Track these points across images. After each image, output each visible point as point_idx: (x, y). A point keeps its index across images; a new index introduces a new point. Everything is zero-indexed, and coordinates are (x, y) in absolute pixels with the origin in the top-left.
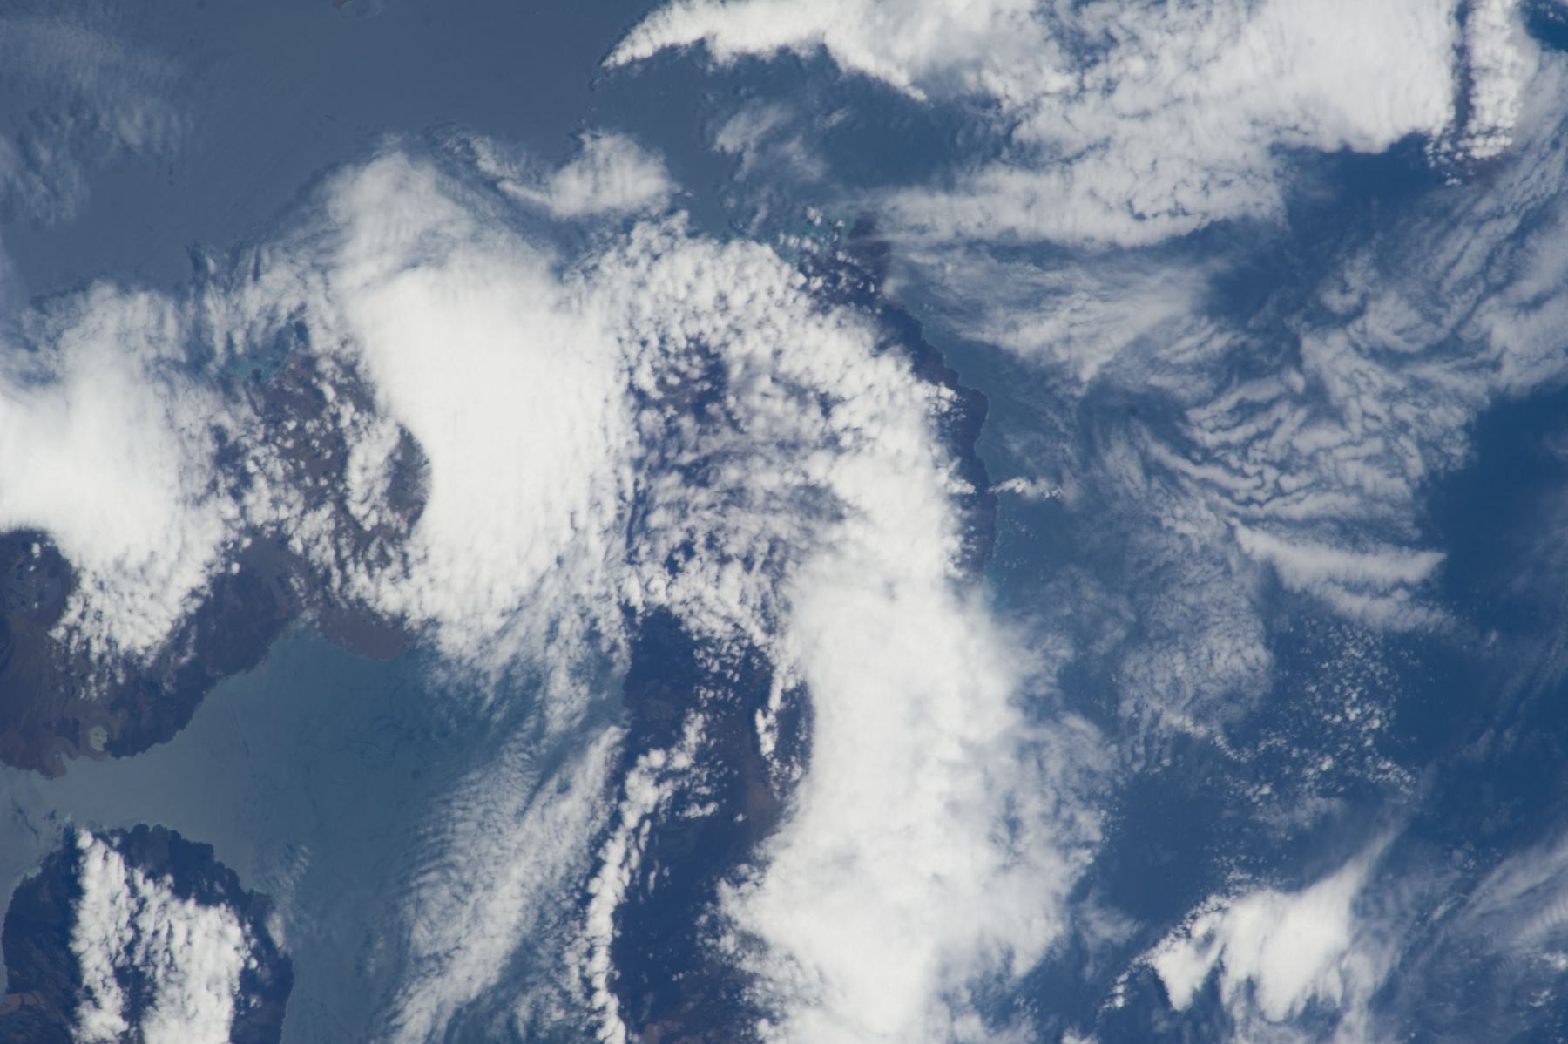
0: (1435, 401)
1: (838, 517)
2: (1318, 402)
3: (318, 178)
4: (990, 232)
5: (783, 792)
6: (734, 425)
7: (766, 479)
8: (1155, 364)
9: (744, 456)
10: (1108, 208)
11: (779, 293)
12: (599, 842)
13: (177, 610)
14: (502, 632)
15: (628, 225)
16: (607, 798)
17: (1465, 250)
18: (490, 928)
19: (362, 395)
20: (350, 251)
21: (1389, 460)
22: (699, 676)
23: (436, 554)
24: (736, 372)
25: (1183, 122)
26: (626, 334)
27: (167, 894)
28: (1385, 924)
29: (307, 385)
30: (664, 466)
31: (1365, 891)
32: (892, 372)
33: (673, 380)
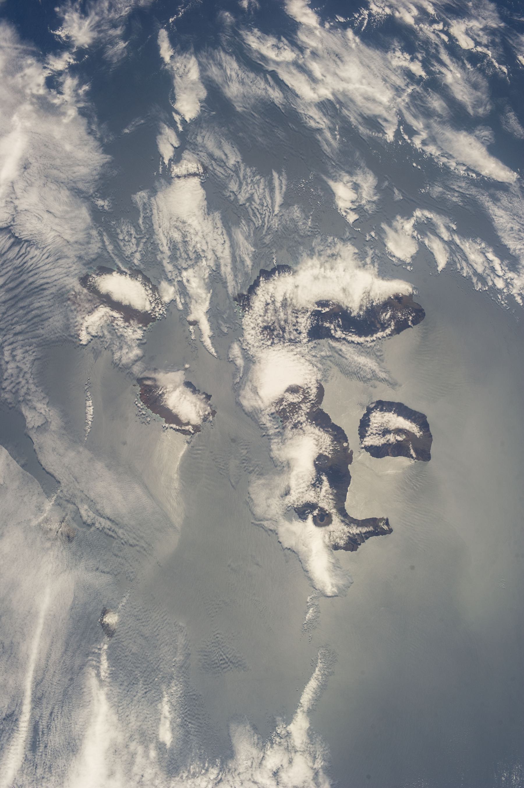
0: (246, 174)
1: (286, 299)
2: (250, 199)
3: (246, 414)
4: (232, 273)
5: (335, 305)
6: (274, 323)
7: (282, 316)
8: (249, 235)
9: (279, 321)
10: (224, 249)
11: (250, 317)
12: (349, 342)
13: (323, 433)
14: (317, 367)
15: (244, 349)
16: (341, 341)
17: (219, 170)
18: (366, 362)
19: (281, 400)
20: (257, 406)
21: (258, 183)
22: (317, 324)
23: (305, 383)
24: (265, 324)
25: (207, 234)
26: (262, 348)
27: (369, 429)
28: (338, 175)
29: (280, 412)
30: (283, 337)
31: (333, 180)
32: (259, 291)
33: (268, 337)
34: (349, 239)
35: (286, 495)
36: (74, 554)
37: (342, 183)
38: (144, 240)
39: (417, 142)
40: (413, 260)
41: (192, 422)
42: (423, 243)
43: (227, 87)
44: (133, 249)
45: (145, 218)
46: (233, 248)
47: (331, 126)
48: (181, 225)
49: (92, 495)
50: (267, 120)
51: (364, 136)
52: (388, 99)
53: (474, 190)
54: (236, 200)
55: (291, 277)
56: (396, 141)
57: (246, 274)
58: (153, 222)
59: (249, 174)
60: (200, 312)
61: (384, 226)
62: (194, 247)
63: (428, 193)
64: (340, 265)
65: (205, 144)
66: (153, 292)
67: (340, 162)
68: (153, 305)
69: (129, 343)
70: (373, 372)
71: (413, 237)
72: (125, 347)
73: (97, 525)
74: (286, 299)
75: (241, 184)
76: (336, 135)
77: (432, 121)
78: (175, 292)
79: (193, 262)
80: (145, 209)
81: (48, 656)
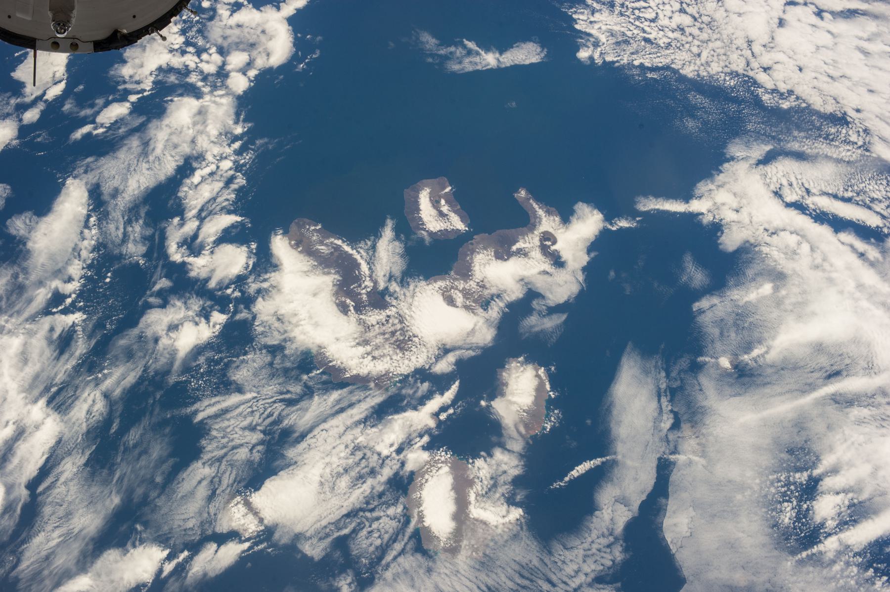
0: (217, 447)
1: (358, 344)
2: (252, 428)
4: (357, 406)
17: (226, 481)
19: (467, 308)
21: (224, 429)
22: (368, 306)
24: (398, 351)
28: (166, 352)
30: (401, 329)
32: (364, 371)
34: (250, 310)
35: (548, 273)
36: (703, 414)
37: (176, 344)
38: (368, 514)
39: (72, 287)
40: (242, 244)
41: (534, 373)
42: (214, 242)
43: (83, 533)
44: (386, 521)
45: (339, 529)
47: (92, 385)
48: (327, 485)
49: (651, 424)
50: (119, 460)
53: (114, 214)
54: (261, 443)
55: (329, 348)
56: (80, 309)
57: (351, 392)
58: (339, 517)
59: (215, 445)
60: (422, 418)
61: (212, 284)
62: (347, 458)
63: (144, 256)
64: (285, 309)
65: (195, 513)
66: (427, 472)
67: (145, 355)
68: (439, 465)
69: (494, 467)
71: (212, 252)
72: (501, 469)
73: (670, 408)
74: (358, 344)
75: (234, 448)
78: (411, 451)
79: (366, 451)
80: (328, 535)
81: (781, 394)
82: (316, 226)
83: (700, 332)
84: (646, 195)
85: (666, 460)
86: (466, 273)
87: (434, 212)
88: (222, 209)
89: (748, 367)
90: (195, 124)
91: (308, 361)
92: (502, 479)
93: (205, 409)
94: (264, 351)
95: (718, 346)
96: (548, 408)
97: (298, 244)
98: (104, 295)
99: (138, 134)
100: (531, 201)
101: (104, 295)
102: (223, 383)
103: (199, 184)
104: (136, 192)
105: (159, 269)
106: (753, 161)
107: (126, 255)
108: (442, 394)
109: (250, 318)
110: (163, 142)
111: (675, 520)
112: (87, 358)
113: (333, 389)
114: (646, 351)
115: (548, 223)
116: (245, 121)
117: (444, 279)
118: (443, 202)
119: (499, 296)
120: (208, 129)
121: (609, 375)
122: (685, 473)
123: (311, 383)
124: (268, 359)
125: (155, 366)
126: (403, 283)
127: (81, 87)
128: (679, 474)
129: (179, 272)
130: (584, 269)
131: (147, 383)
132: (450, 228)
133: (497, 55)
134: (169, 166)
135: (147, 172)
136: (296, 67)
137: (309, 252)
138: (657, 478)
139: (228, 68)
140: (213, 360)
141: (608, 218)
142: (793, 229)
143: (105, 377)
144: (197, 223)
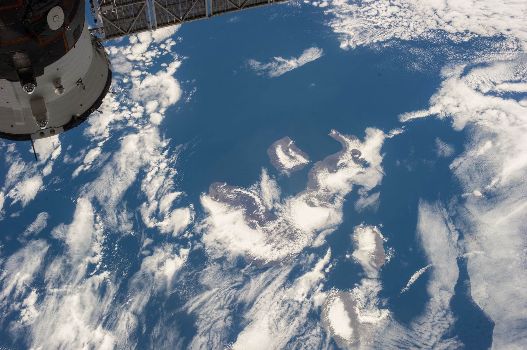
2: (221, 308)
4: (277, 278)
19: (322, 205)
21: (206, 313)
22: (266, 220)
24: (291, 241)
30: (289, 228)
32: (275, 258)
34: (200, 242)
35: (361, 173)
40: (185, 207)
41: (371, 231)
42: (169, 210)
46: (262, 290)
47: (125, 309)
49: (446, 240)
51: (116, 288)
52: (73, 296)
53: (109, 211)
54: (229, 315)
55: (251, 251)
56: (106, 269)
57: (271, 272)
60: (316, 274)
61: (175, 234)
62: (280, 309)
63: (132, 229)
64: (220, 236)
66: (327, 304)
67: (149, 285)
68: (334, 298)
70: (267, 181)
71: (170, 216)
72: (369, 290)
73: (454, 228)
76: (130, 302)
77: (72, 263)
78: (315, 295)
79: (290, 302)
82: (223, 184)
83: (458, 180)
84: (403, 113)
85: (462, 258)
86: (315, 186)
87: (287, 158)
88: (168, 190)
89: (492, 192)
90: (139, 148)
91: (242, 261)
92: (371, 296)
93: (192, 305)
94: (215, 263)
95: (471, 185)
96: (385, 249)
97: (216, 198)
98: (117, 258)
99: (109, 163)
100: (340, 135)
101: (117, 258)
102: (197, 287)
103: (151, 180)
104: (118, 195)
105: (143, 234)
106: (458, 76)
107: (122, 232)
108: (323, 258)
109: (202, 247)
110: (124, 163)
111: (477, 291)
112: (118, 295)
113: (260, 273)
114: (431, 199)
115: (353, 144)
116: (166, 138)
117: (305, 193)
118: (290, 150)
119: (338, 194)
120: (147, 149)
121: (414, 219)
122: (474, 262)
123: (247, 273)
124: (219, 266)
125: (156, 289)
126: (282, 202)
127: (70, 146)
128: (472, 264)
129: (154, 233)
130: (381, 164)
131: (155, 299)
132: (299, 164)
133: (296, 60)
134: (132, 176)
135: (120, 182)
136: (185, 100)
137: (224, 200)
138: (459, 270)
139: (148, 112)
140: (188, 276)
141: (386, 132)
142: (492, 107)
143: (131, 303)
144: (157, 203)
